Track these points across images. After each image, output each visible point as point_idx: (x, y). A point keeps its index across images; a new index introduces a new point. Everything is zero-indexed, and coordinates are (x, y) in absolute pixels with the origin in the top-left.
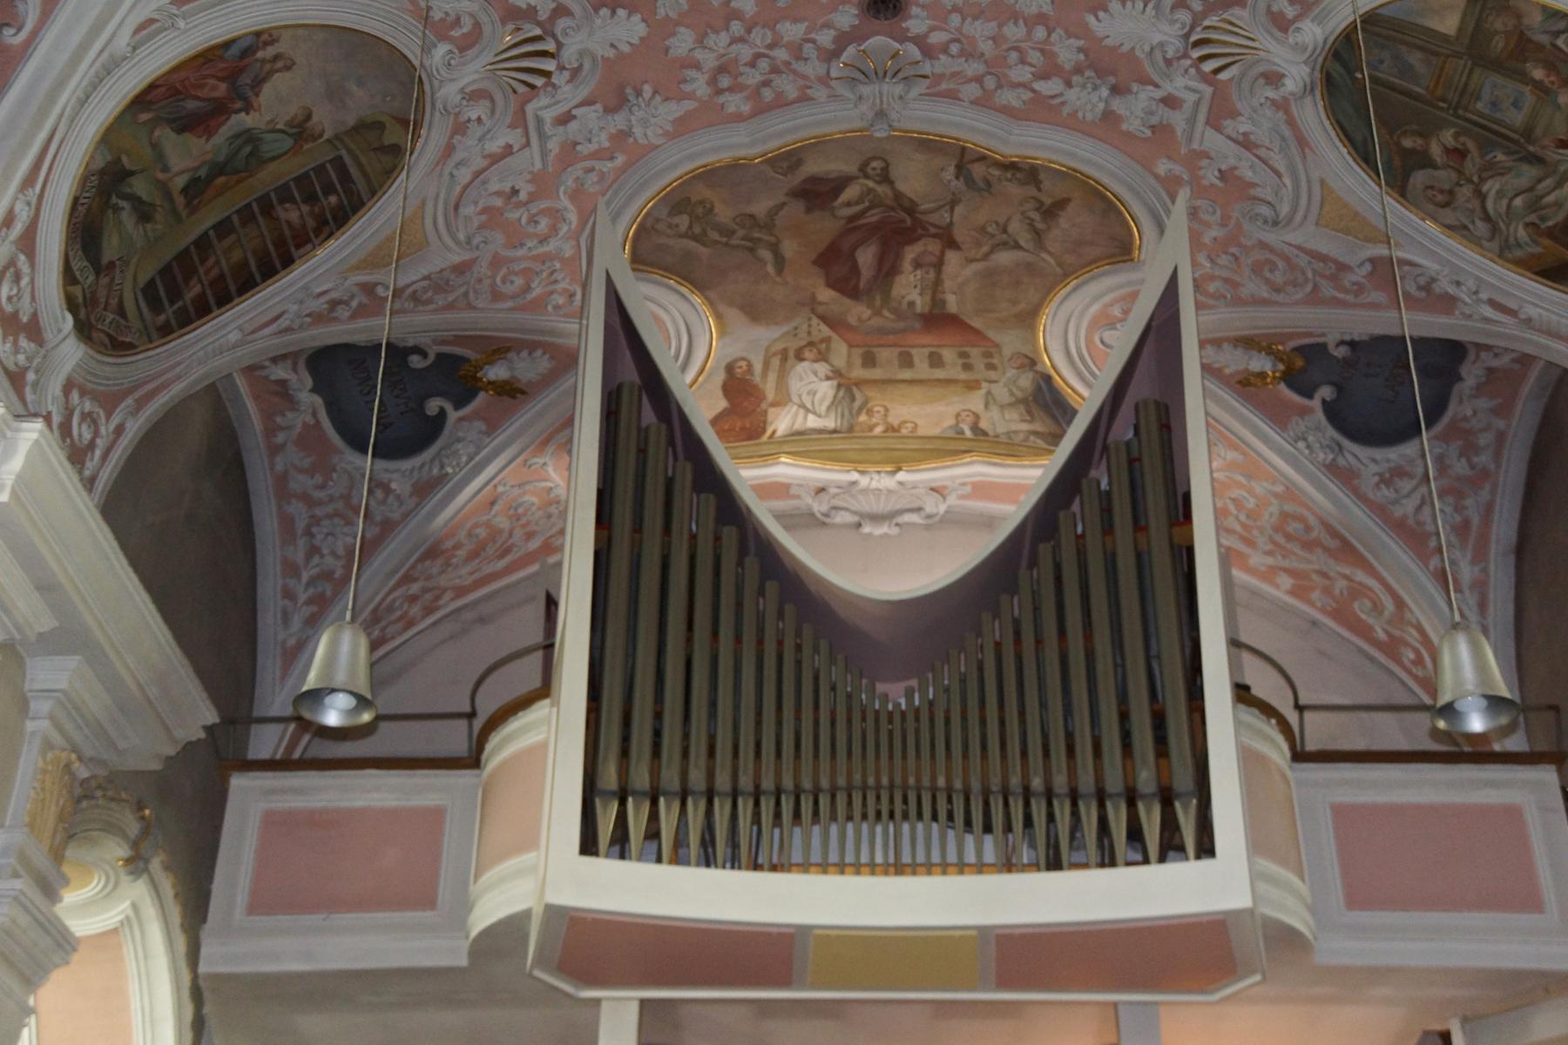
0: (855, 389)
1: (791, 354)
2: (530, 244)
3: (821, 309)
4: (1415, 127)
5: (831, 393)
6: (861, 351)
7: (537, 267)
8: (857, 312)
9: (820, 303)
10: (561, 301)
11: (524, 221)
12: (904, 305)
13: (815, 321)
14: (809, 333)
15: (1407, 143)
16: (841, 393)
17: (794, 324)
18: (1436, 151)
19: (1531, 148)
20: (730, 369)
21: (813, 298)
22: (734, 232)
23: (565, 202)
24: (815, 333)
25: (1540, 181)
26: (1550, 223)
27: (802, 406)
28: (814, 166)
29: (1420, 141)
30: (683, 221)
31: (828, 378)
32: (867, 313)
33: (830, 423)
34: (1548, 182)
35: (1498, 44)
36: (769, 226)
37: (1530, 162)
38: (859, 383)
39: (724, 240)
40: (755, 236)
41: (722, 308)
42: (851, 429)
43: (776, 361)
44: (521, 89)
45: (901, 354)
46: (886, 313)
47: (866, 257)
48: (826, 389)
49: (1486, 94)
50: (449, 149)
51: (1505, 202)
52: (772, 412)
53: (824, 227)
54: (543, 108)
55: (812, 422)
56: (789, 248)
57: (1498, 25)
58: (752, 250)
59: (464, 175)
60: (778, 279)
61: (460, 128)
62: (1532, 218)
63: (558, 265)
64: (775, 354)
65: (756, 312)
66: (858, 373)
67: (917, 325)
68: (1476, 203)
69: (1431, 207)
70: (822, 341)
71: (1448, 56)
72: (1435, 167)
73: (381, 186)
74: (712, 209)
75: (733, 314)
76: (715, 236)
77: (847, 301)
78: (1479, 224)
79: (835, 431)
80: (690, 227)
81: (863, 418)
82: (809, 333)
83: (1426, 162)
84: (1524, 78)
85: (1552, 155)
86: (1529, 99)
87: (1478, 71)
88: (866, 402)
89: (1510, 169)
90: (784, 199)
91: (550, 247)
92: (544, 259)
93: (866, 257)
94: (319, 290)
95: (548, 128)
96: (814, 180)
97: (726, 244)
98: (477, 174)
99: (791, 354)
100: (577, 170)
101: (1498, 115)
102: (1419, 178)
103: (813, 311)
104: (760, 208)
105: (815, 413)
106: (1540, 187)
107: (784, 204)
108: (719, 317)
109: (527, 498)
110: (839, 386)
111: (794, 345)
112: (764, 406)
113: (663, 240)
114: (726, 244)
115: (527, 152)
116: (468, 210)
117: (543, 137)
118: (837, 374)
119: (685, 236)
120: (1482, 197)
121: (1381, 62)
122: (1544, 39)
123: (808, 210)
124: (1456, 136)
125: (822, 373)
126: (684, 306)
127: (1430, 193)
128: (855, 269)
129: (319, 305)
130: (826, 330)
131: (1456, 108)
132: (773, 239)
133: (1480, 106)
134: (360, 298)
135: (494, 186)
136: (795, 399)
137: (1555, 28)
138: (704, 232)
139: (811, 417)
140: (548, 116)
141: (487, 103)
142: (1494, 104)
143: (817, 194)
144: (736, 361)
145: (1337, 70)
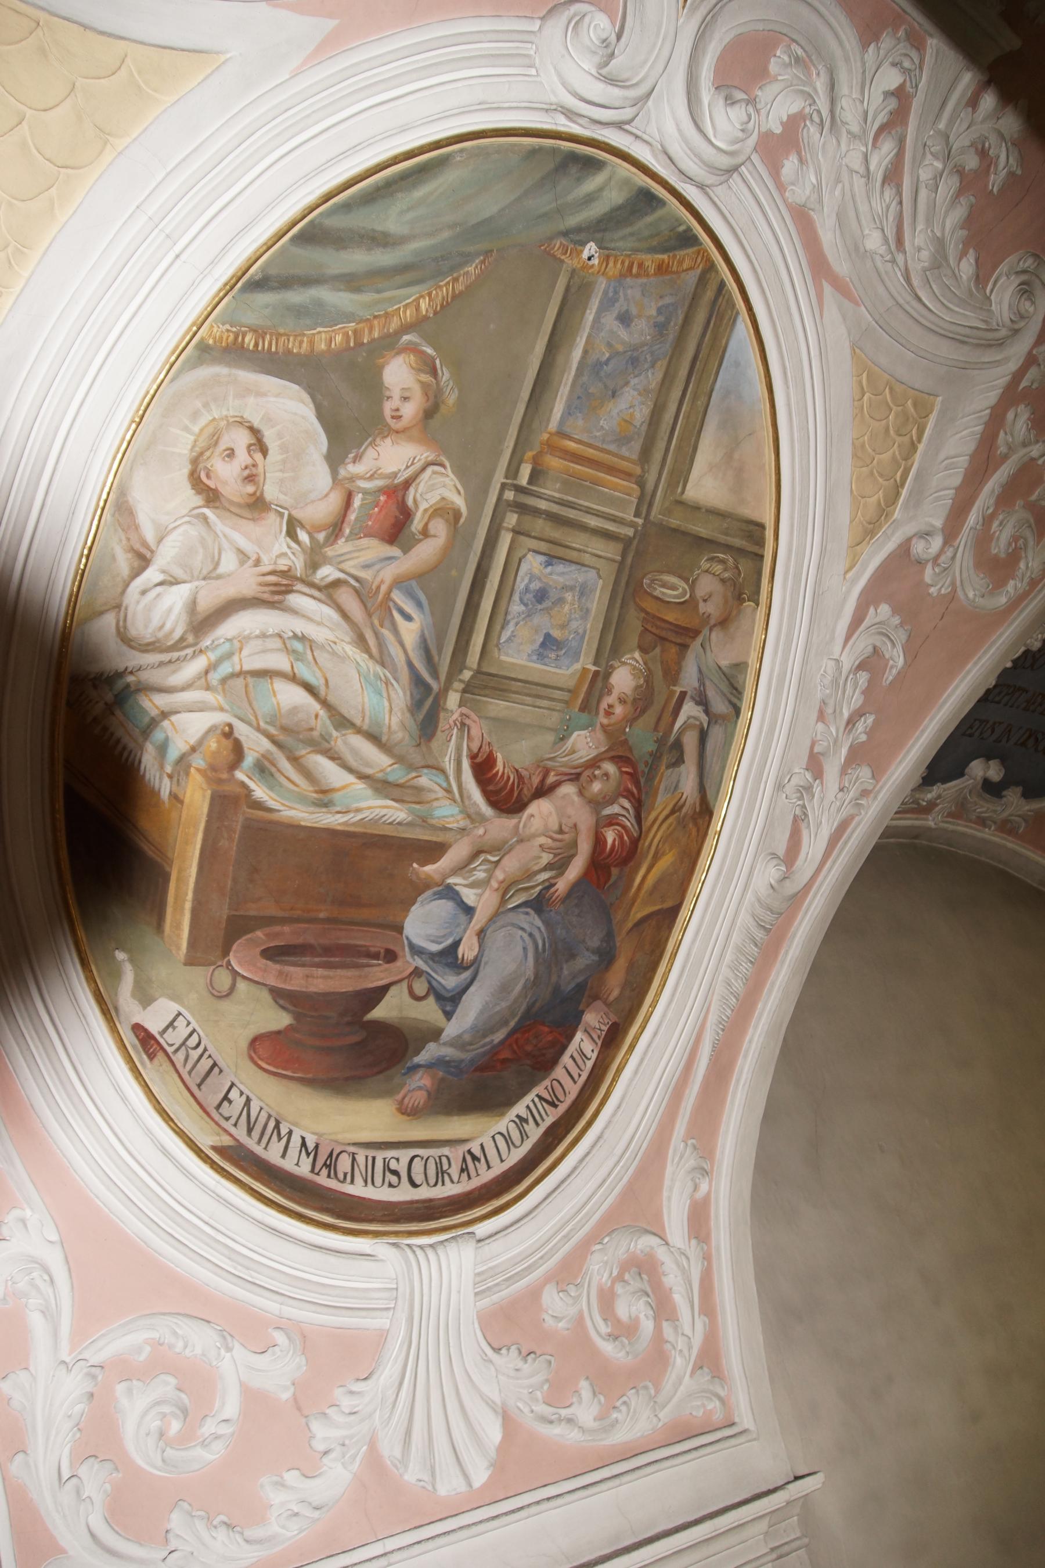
4: (451, 398)
15: (398, 374)
18: (390, 458)
19: (453, 699)
25: (374, 738)
26: (260, 792)
29: (410, 411)
34: (379, 760)
35: (672, 589)
37: (416, 706)
49: (561, 575)
51: (281, 662)
57: (707, 585)
62: (255, 744)
68: (247, 583)
69: (182, 444)
71: (641, 483)
72: (334, 460)
78: (176, 598)
83: (348, 426)
84: (609, 651)
85: (452, 751)
86: (566, 672)
87: (611, 551)
89: (383, 659)
101: (516, 608)
102: (287, 409)
106: (358, 742)
120: (277, 592)
121: (625, 319)
122: (689, 678)
124: (444, 511)
127: (241, 439)
131: (522, 509)
133: (533, 563)
137: (711, 693)
142: (541, 596)
145: (608, 187)
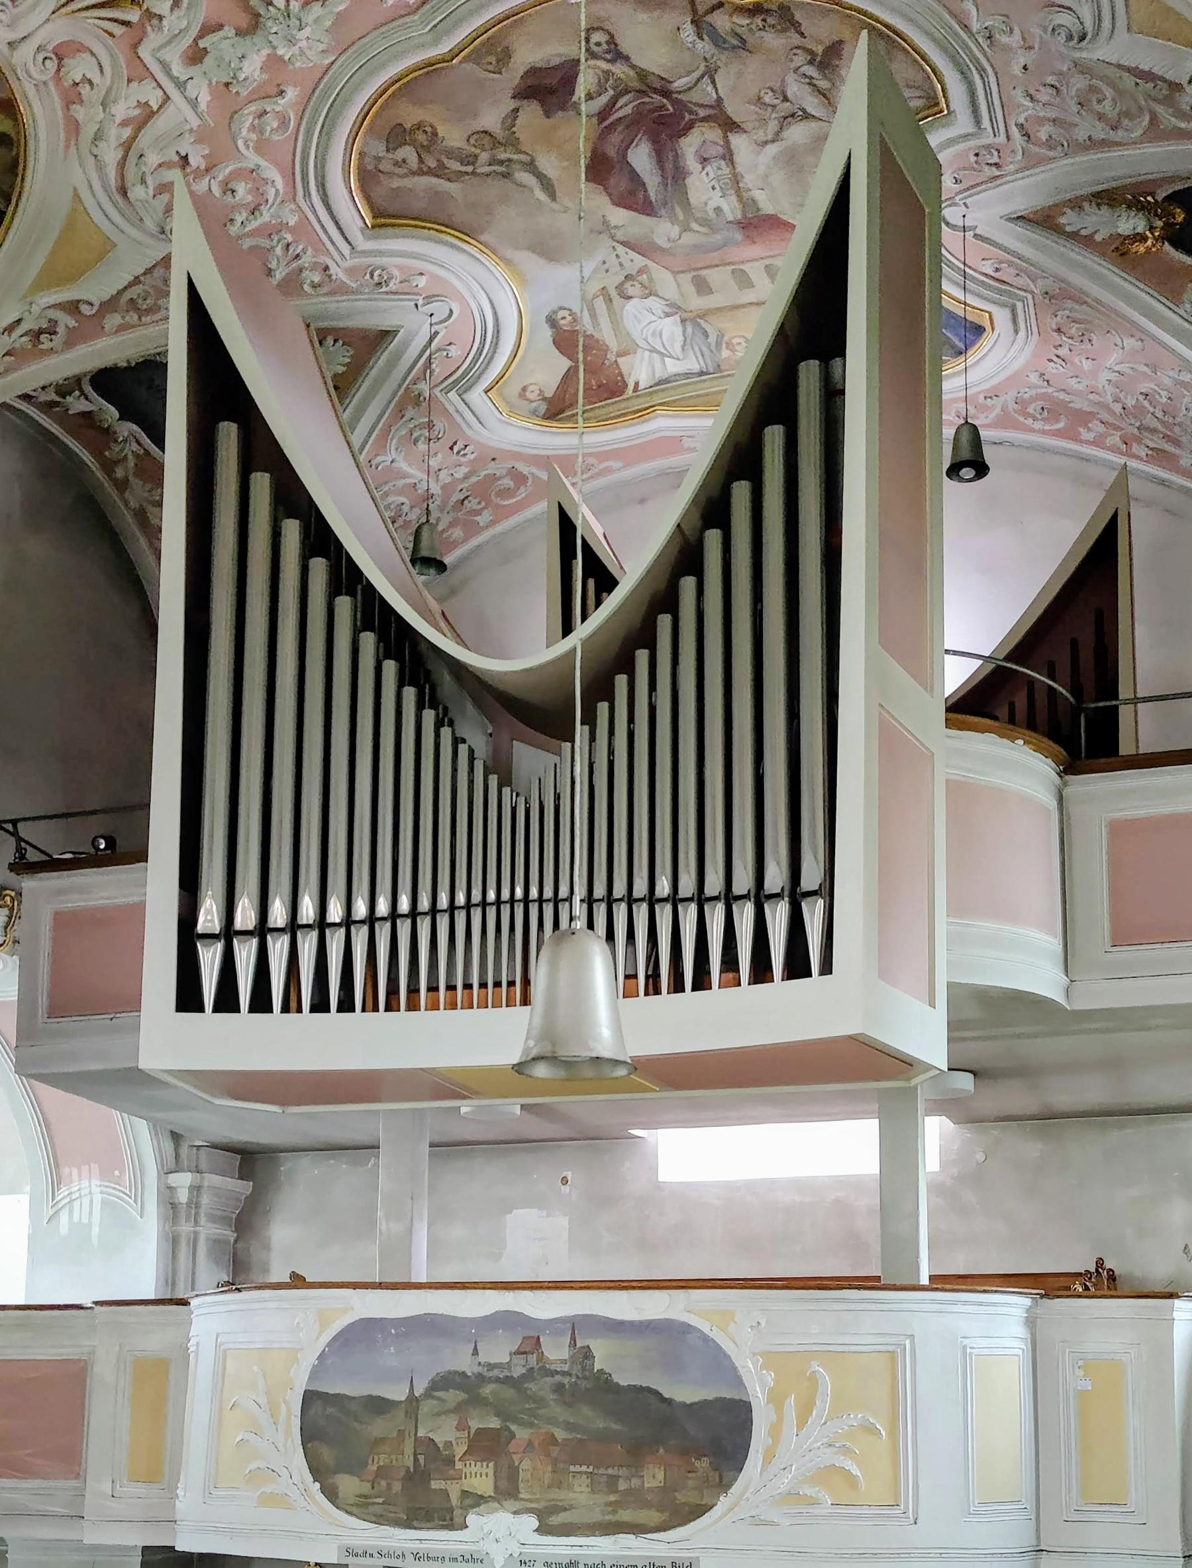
0: (702, 322)
1: (613, 293)
2: (239, 219)
3: (620, 235)
5: (678, 330)
6: (689, 276)
7: (266, 243)
8: (663, 230)
9: (616, 227)
10: (317, 278)
11: (216, 191)
12: (712, 214)
13: (621, 250)
14: (621, 265)
16: (689, 330)
17: (600, 258)
20: (552, 322)
21: (605, 222)
22: (476, 156)
23: (253, 159)
24: (627, 264)
27: (653, 350)
28: (531, 53)
30: (407, 153)
31: (667, 315)
32: (675, 231)
33: (692, 364)
36: (513, 142)
38: (704, 314)
39: (470, 169)
40: (500, 156)
41: (509, 253)
42: (718, 368)
43: (600, 304)
44: (118, 30)
45: (733, 272)
46: (695, 226)
47: (641, 157)
48: (671, 328)
50: (74, 127)
52: (620, 360)
53: (579, 132)
54: (164, 48)
55: (672, 367)
56: (549, 164)
58: (506, 176)
59: (111, 156)
60: (555, 206)
61: (72, 96)
63: (289, 238)
64: (595, 297)
65: (548, 249)
66: (697, 303)
67: (738, 236)
70: (641, 271)
73: (12, 187)
74: (435, 134)
75: (528, 260)
76: (455, 166)
77: (645, 219)
79: (702, 373)
80: (421, 160)
81: (725, 353)
82: (621, 265)
88: (721, 336)
90: (513, 104)
91: (266, 216)
92: (269, 231)
93: (641, 157)
94: (5, 324)
95: (178, 69)
96: (533, 72)
97: (473, 173)
98: (127, 146)
99: (613, 293)
100: (247, 119)
103: (613, 237)
104: (491, 119)
105: (671, 357)
107: (516, 110)
108: (508, 262)
109: (390, 499)
110: (683, 321)
111: (612, 281)
112: (611, 357)
113: (396, 183)
114: (473, 173)
115: (170, 109)
116: (137, 193)
117: (181, 85)
118: (674, 309)
119: (420, 172)
123: (548, 115)
125: (659, 312)
126: (462, 257)
128: (634, 177)
129: (18, 339)
130: (640, 261)
132: (523, 157)
134: (66, 321)
135: (153, 159)
136: (641, 343)
138: (442, 166)
139: (667, 359)
140: (174, 57)
141: (86, 56)
143: (548, 89)
144: (555, 312)
